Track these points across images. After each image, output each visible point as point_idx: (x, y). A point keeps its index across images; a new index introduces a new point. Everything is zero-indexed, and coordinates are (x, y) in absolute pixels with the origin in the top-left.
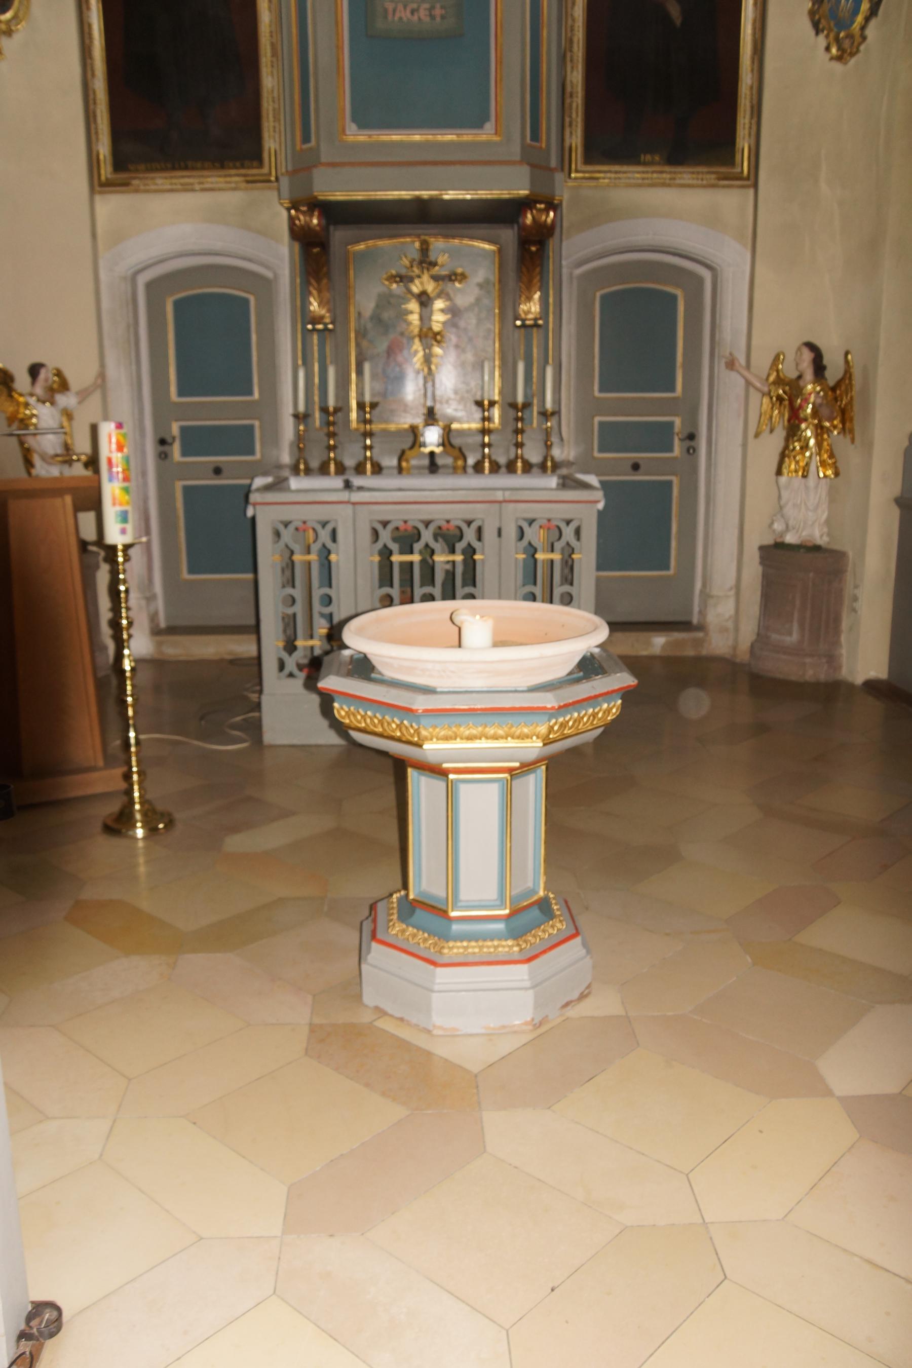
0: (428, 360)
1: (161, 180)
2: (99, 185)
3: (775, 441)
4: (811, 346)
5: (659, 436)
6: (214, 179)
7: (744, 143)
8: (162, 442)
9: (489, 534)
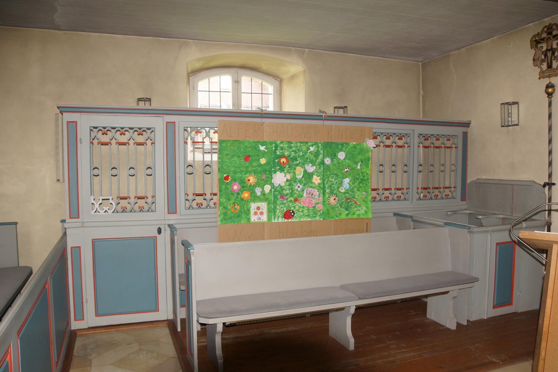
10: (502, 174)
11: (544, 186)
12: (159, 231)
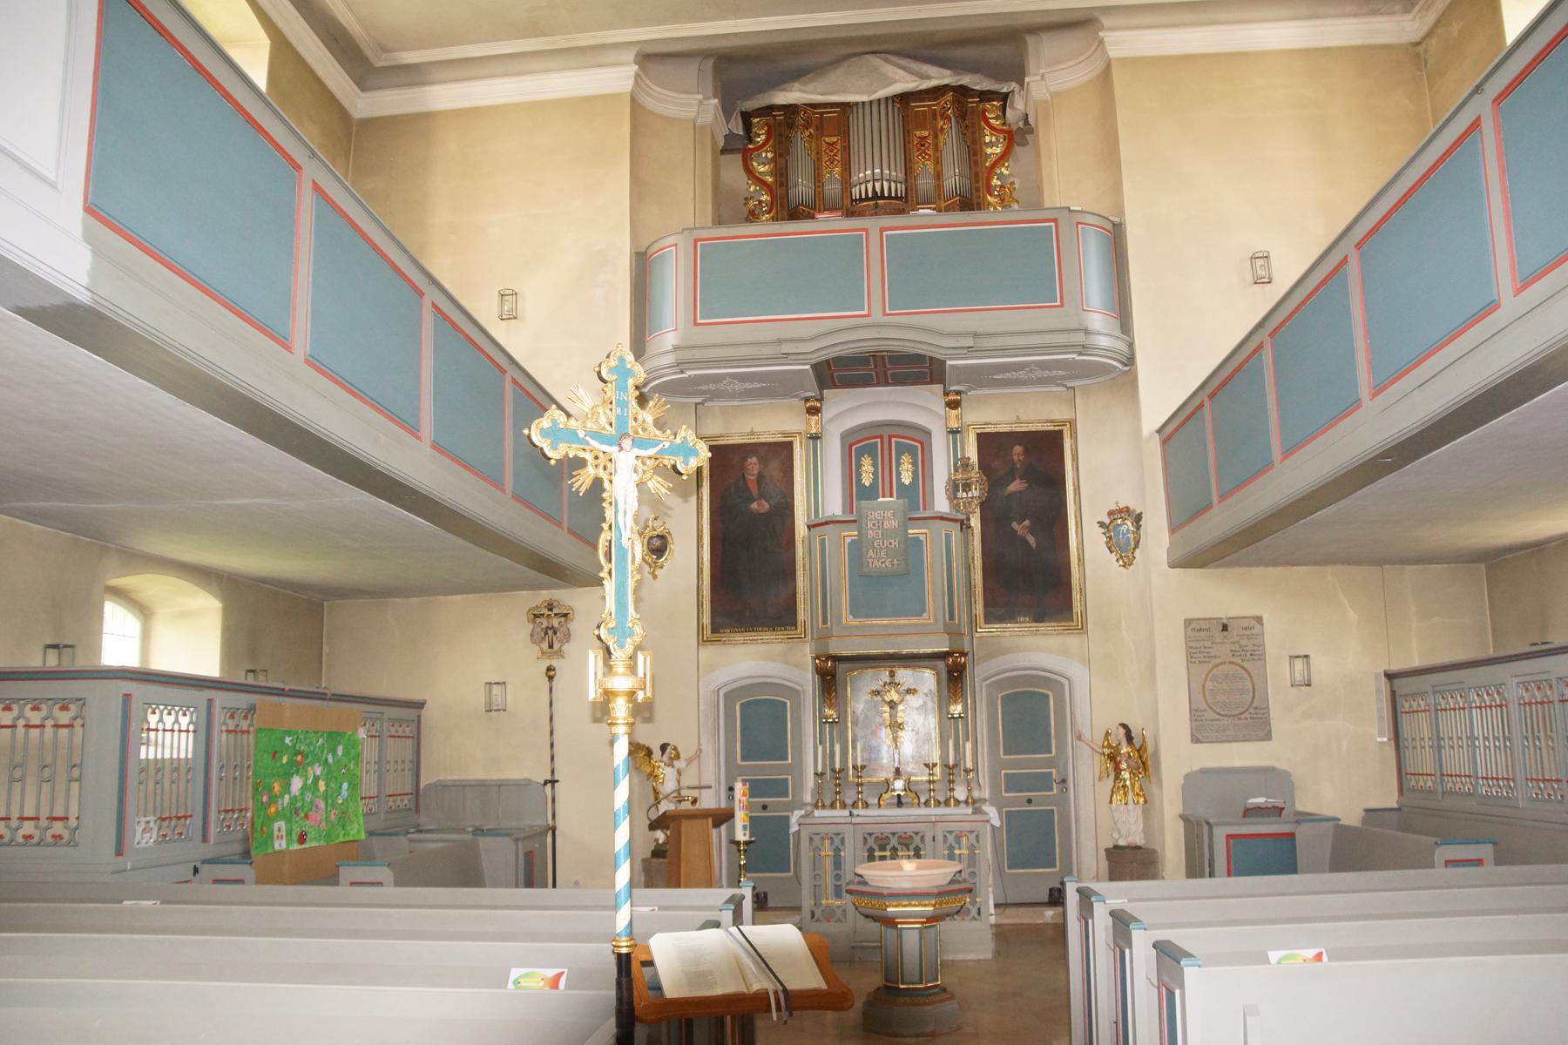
0: (895, 739)
1: (739, 637)
2: (703, 641)
3: (1110, 782)
4: (1124, 726)
5: (1043, 782)
6: (768, 636)
7: (1077, 606)
9: (928, 839)
10: (477, 773)
11: (546, 783)
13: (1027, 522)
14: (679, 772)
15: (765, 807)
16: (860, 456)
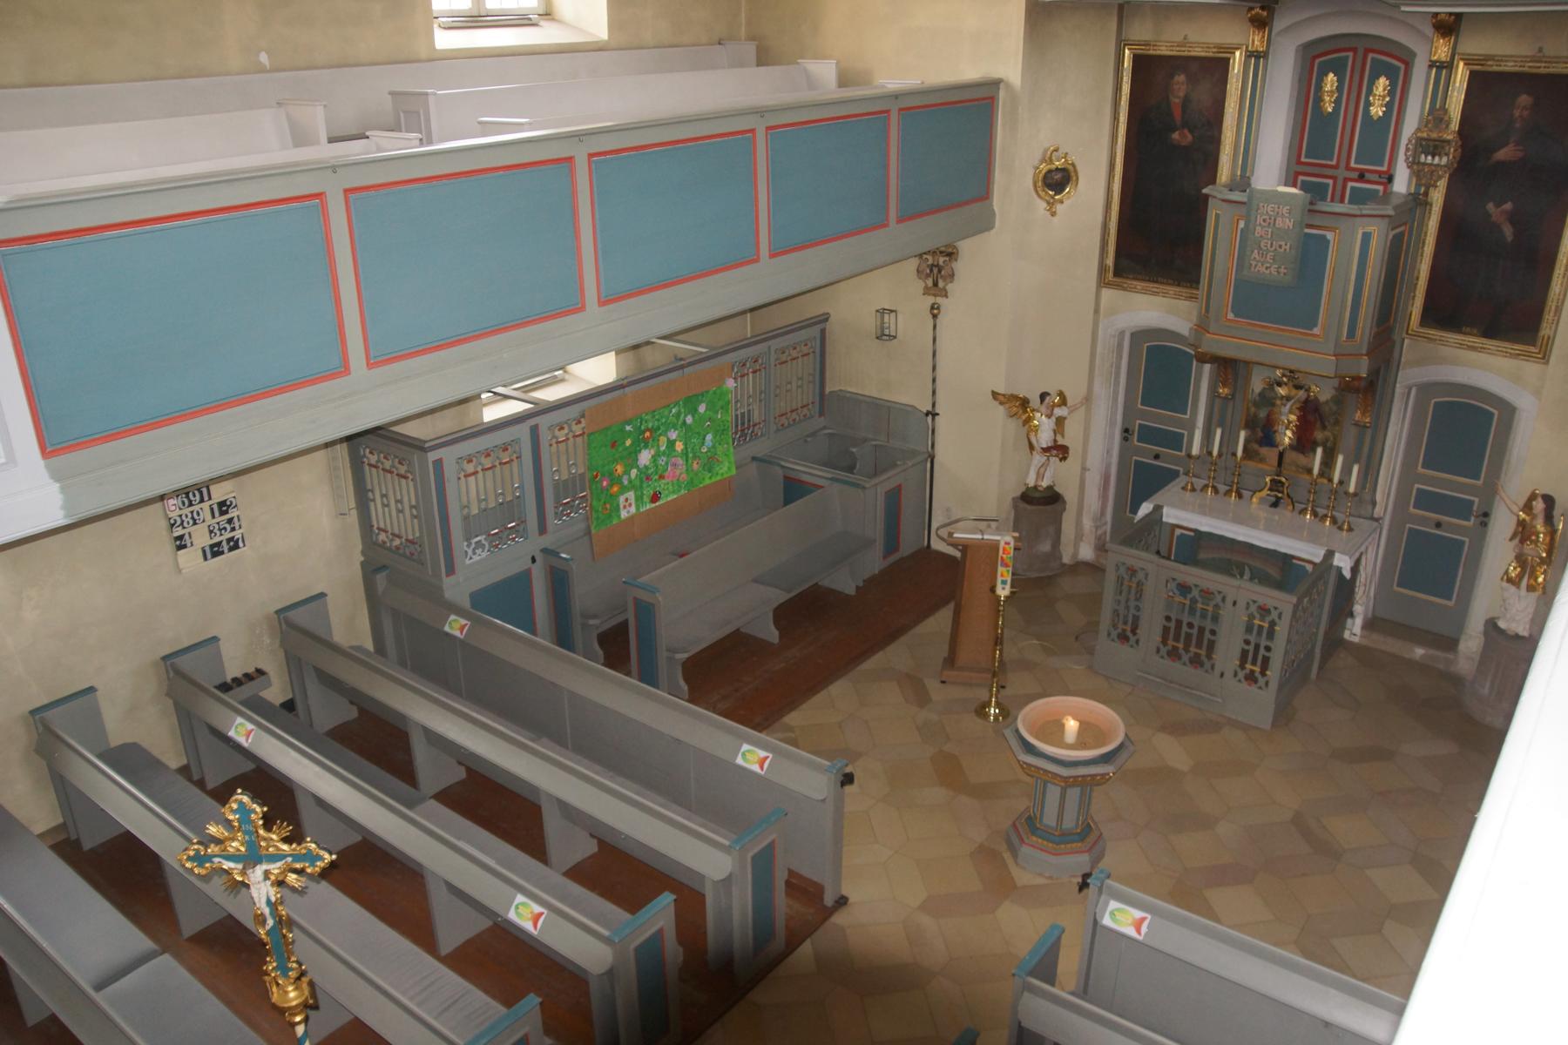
1: (1140, 285)
2: (1102, 282)
5: (1463, 509)
8: (1126, 431)
10: (872, 390)
11: (927, 414)
12: (534, 560)
13: (1508, 206)
14: (1060, 422)
15: (1157, 457)
16: (1323, 74)
